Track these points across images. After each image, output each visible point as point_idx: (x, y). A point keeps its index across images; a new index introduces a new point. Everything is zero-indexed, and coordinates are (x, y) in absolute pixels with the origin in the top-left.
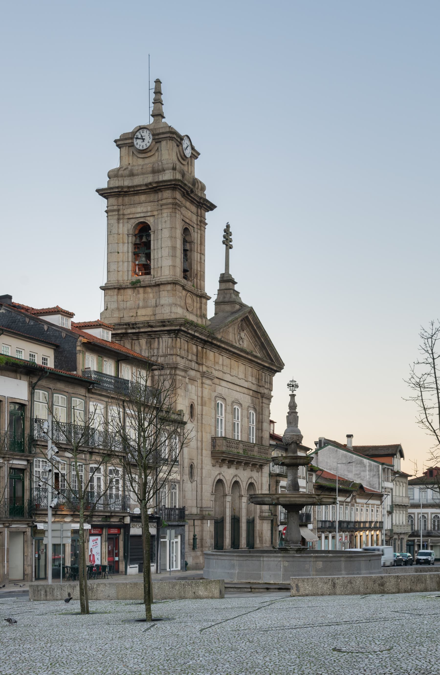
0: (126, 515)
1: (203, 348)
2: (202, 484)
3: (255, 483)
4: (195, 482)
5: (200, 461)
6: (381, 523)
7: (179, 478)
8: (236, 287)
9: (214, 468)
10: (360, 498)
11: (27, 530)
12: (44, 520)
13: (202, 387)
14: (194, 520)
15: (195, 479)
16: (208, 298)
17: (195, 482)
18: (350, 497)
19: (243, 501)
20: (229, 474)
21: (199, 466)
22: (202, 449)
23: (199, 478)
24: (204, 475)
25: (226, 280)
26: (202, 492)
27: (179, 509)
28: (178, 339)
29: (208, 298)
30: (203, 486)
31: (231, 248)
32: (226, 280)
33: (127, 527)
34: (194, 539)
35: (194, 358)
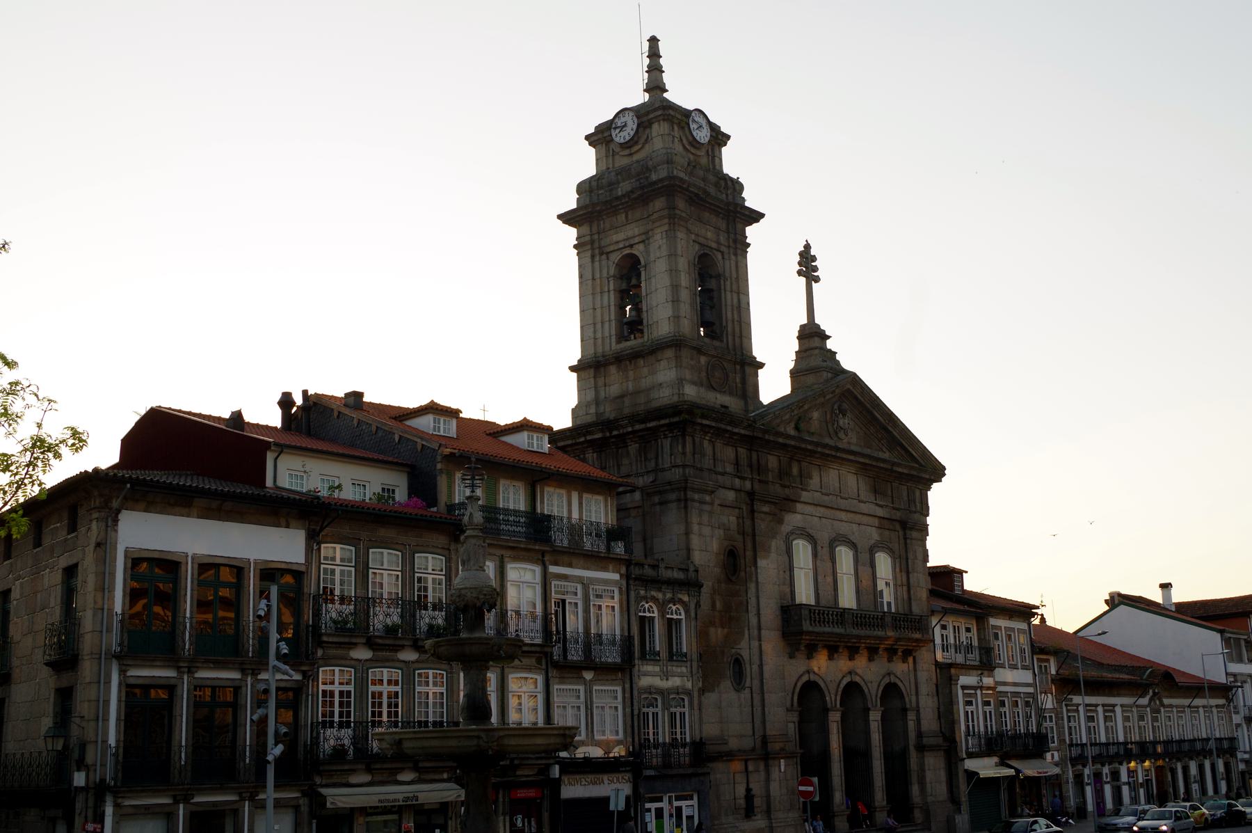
0: (552, 761)
1: (750, 450)
2: (763, 693)
3: (900, 684)
4: (747, 691)
5: (756, 651)
6: (1232, 740)
7: (689, 685)
8: (830, 344)
9: (793, 661)
10: (1167, 697)
11: (301, 802)
12: (344, 781)
13: (753, 519)
14: (746, 761)
15: (748, 684)
16: (761, 365)
17: (747, 691)
18: (1148, 697)
19: (871, 718)
20: (828, 669)
21: (756, 659)
22: (759, 629)
23: (756, 683)
24: (766, 675)
25: (812, 336)
26: (763, 706)
27: (693, 743)
28: (689, 439)
29: (761, 365)
30: (766, 696)
31: (817, 280)
32: (812, 336)
33: (557, 784)
34: (749, 796)
35: (730, 469)
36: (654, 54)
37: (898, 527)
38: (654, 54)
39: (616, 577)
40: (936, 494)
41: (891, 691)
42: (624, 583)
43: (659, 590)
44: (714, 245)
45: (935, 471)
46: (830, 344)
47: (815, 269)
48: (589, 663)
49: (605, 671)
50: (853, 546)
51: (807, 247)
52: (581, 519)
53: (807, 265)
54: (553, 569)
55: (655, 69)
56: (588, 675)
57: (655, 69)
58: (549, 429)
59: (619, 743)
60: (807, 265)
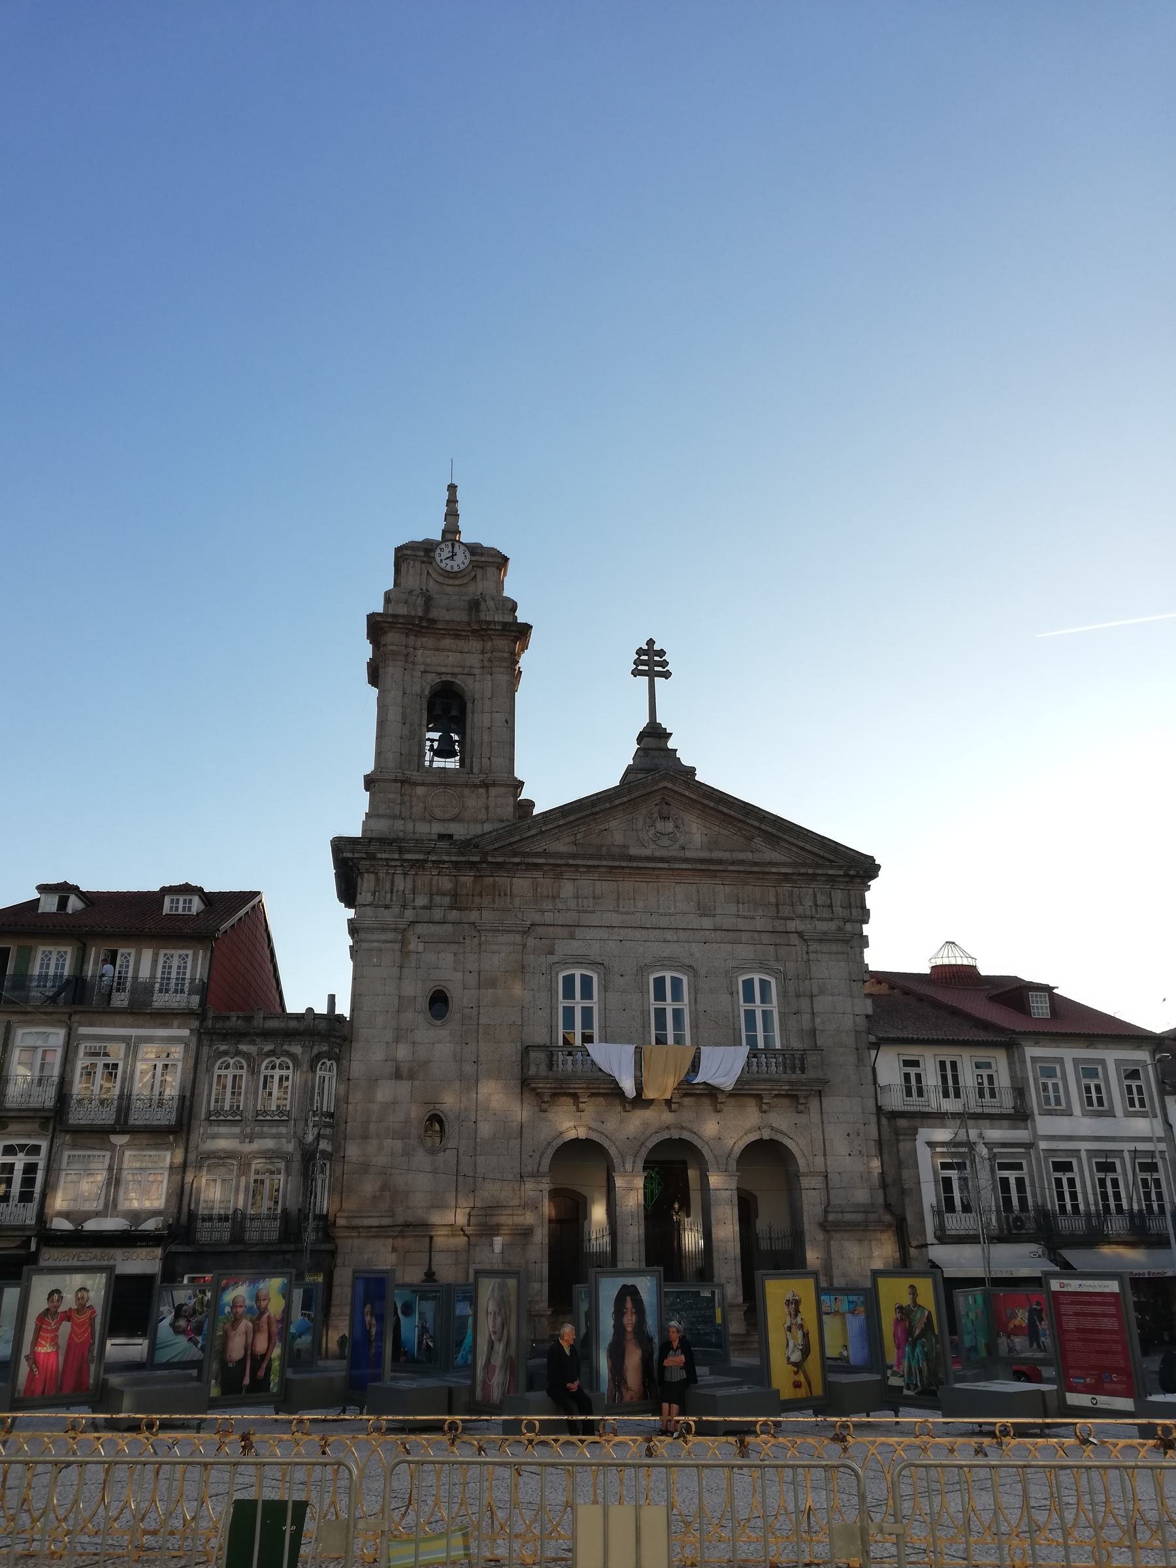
32: (654, 737)
36: (452, 501)
37: (794, 939)
38: (452, 501)
39: (186, 1032)
40: (875, 896)
41: (766, 1154)
42: (194, 1039)
43: (253, 1042)
44: (457, 670)
45: (862, 869)
46: (671, 745)
47: (664, 664)
48: (122, 1123)
49: (155, 1135)
50: (691, 969)
51: (651, 642)
52: (153, 976)
53: (651, 663)
54: (83, 1030)
55: (452, 514)
56: (119, 1140)
57: (452, 514)
58: (201, 889)
59: (154, 1213)
60: (651, 663)
